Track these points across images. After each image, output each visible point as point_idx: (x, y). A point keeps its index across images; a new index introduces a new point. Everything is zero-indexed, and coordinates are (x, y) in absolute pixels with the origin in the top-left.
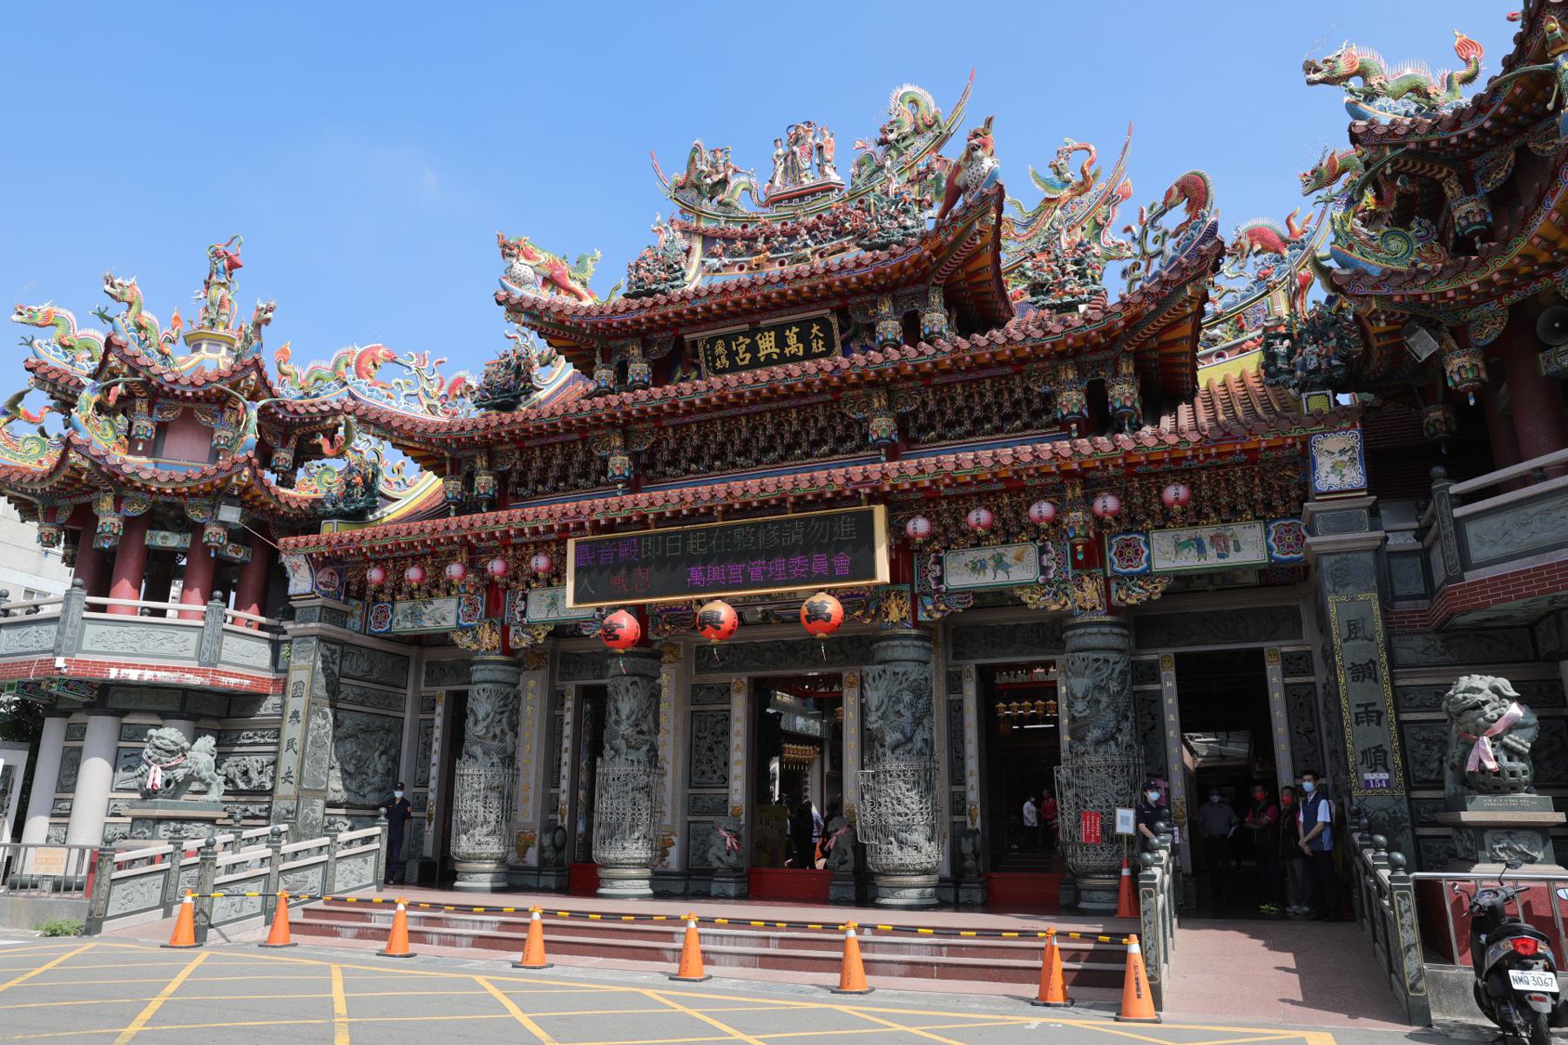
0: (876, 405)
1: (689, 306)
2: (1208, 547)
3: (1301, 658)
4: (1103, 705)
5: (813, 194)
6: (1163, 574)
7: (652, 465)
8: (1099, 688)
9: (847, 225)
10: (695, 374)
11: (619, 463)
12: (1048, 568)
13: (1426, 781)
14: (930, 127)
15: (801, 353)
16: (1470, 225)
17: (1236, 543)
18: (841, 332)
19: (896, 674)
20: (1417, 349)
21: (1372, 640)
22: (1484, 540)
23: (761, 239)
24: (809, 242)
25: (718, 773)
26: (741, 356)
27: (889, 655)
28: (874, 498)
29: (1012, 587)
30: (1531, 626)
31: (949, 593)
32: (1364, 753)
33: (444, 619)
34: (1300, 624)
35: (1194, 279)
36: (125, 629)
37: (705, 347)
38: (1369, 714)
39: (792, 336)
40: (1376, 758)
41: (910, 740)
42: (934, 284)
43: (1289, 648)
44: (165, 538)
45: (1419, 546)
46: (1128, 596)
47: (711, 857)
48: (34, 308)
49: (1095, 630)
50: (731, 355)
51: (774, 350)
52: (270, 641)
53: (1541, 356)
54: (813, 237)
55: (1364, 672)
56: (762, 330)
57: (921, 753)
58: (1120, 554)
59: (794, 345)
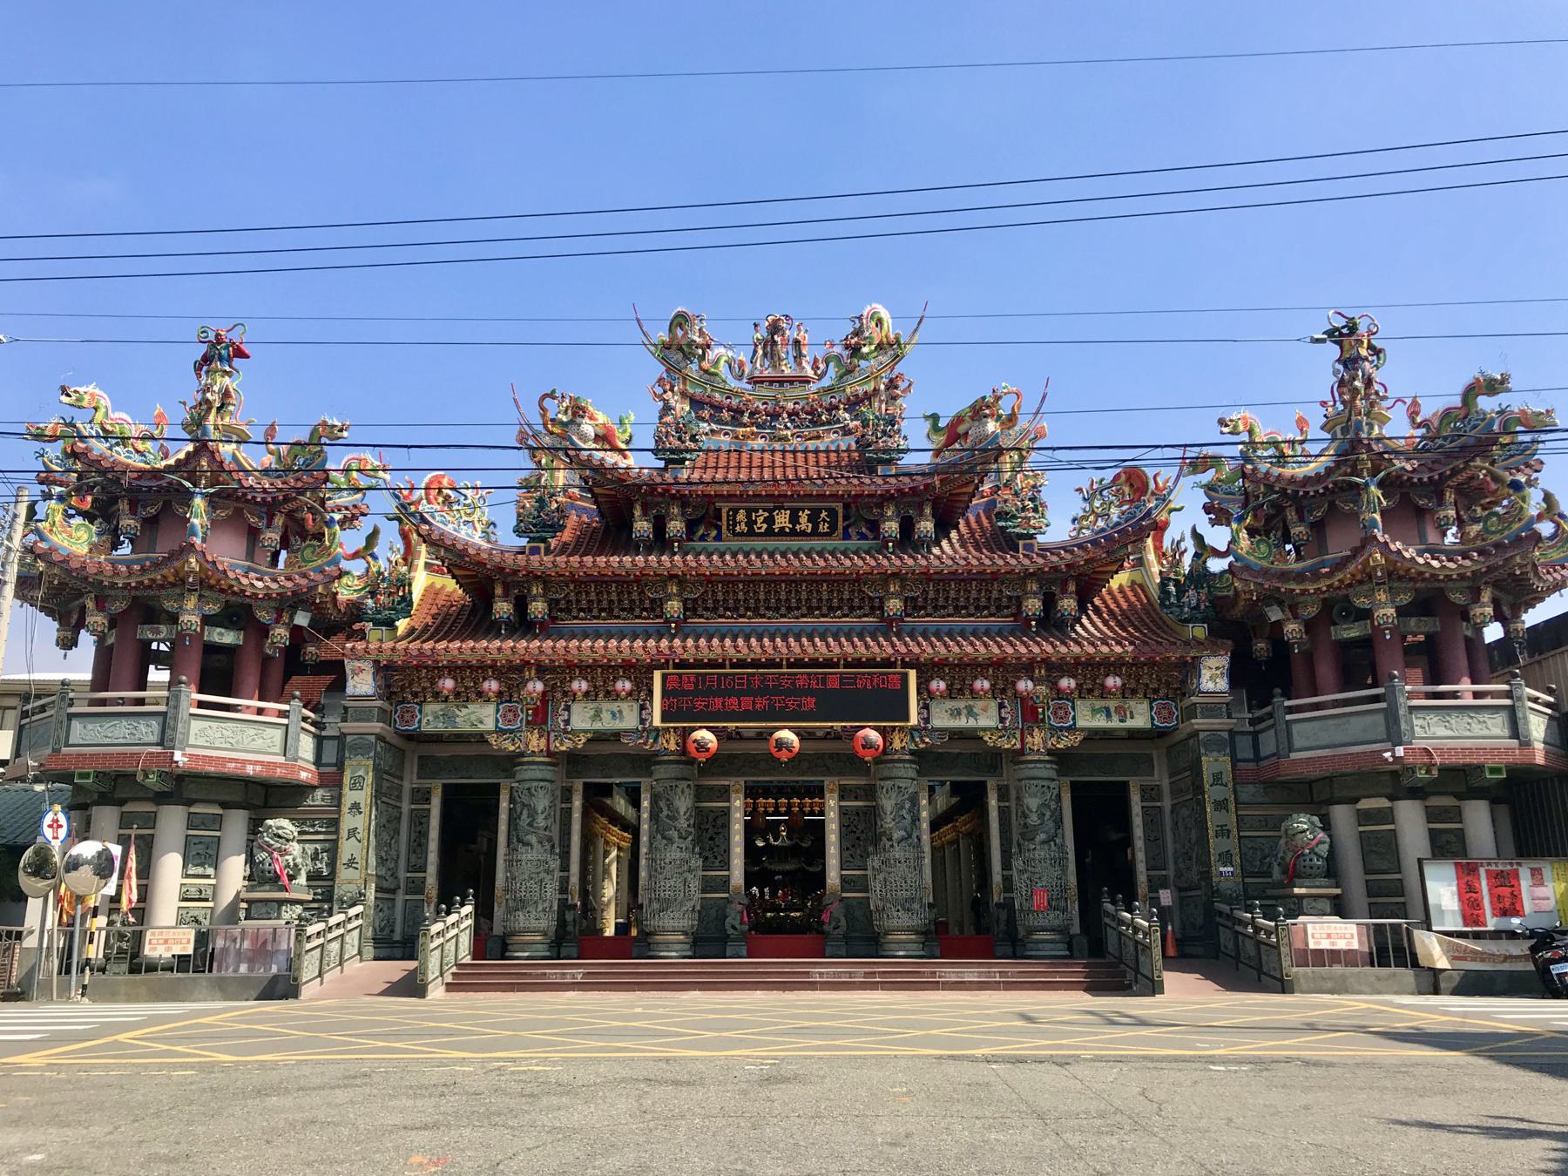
1: (742, 488)
2: (1113, 714)
3: (1152, 789)
4: (1047, 817)
5: (791, 382)
6: (1082, 730)
7: (694, 610)
9: (823, 417)
10: (714, 533)
11: (674, 607)
12: (1005, 719)
13: (1253, 872)
15: (809, 531)
16: (1300, 540)
17: (1131, 713)
18: (844, 520)
19: (899, 788)
20: (1269, 614)
21: (1226, 786)
22: (1301, 735)
24: (789, 424)
25: (720, 858)
26: (759, 525)
27: (895, 773)
28: (906, 665)
29: (976, 729)
30: (1310, 783)
31: (934, 730)
32: (1220, 855)
33: (481, 722)
35: (1134, 542)
36: (223, 725)
37: (728, 512)
38: (1223, 832)
39: (804, 517)
40: (1226, 858)
41: (910, 836)
42: (927, 500)
43: (1147, 780)
44: (221, 634)
45: (1251, 729)
46: (1058, 743)
47: (728, 926)
48: (81, 390)
49: (1042, 766)
50: (751, 523)
51: (787, 525)
52: (315, 736)
53: (1332, 628)
54: (792, 421)
55: (1221, 805)
56: (783, 508)
58: (1055, 713)
59: (804, 523)
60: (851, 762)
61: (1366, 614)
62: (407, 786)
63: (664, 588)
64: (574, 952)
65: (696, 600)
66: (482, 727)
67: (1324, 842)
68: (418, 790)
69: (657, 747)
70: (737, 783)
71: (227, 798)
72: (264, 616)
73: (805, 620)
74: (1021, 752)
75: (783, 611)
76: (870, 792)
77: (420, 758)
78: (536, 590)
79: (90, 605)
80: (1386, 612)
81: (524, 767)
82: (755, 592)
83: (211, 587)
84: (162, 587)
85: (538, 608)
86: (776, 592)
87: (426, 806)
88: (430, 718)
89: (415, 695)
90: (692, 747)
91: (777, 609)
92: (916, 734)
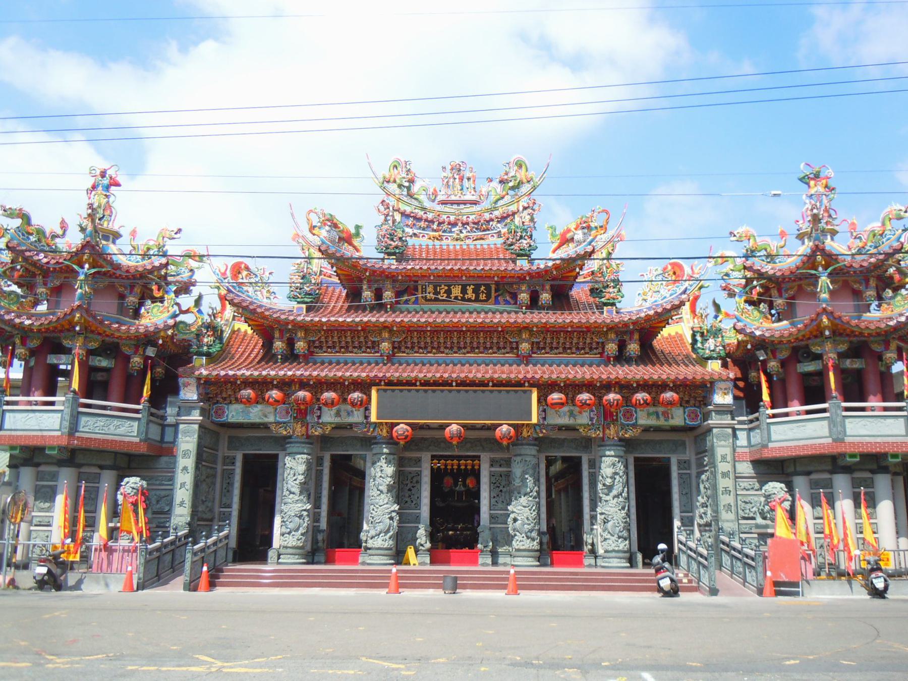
0: (524, 337)
6: (641, 426)
7: (400, 348)
8: (616, 473)
12: (593, 418)
14: (529, 182)
15: (473, 299)
17: (672, 415)
19: (526, 461)
23: (436, 224)
27: (523, 452)
31: (548, 425)
34: (686, 448)
39: (470, 290)
44: (100, 361)
51: (460, 294)
57: (535, 498)
58: (624, 415)
59: (470, 294)
60: (494, 444)
61: (819, 357)
62: (220, 454)
63: (380, 334)
64: (323, 559)
65: (400, 342)
66: (266, 420)
67: (788, 500)
68: (228, 457)
69: (375, 434)
70: (426, 457)
71: (103, 463)
72: (126, 350)
73: (469, 355)
74: (603, 439)
75: (455, 349)
76: (508, 462)
77: (229, 437)
78: (301, 334)
79: (18, 341)
80: (831, 357)
81: (292, 445)
82: (438, 337)
83: (92, 332)
84: (61, 331)
85: (300, 346)
86: (451, 338)
87: (233, 467)
88: (234, 413)
89: (225, 399)
90: (395, 434)
91: (452, 348)
92: (537, 428)
